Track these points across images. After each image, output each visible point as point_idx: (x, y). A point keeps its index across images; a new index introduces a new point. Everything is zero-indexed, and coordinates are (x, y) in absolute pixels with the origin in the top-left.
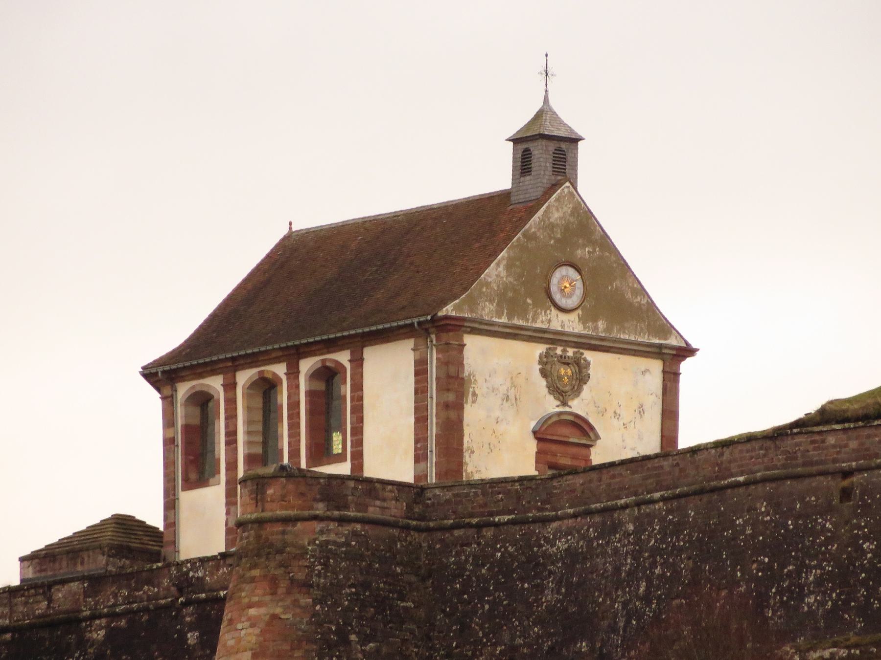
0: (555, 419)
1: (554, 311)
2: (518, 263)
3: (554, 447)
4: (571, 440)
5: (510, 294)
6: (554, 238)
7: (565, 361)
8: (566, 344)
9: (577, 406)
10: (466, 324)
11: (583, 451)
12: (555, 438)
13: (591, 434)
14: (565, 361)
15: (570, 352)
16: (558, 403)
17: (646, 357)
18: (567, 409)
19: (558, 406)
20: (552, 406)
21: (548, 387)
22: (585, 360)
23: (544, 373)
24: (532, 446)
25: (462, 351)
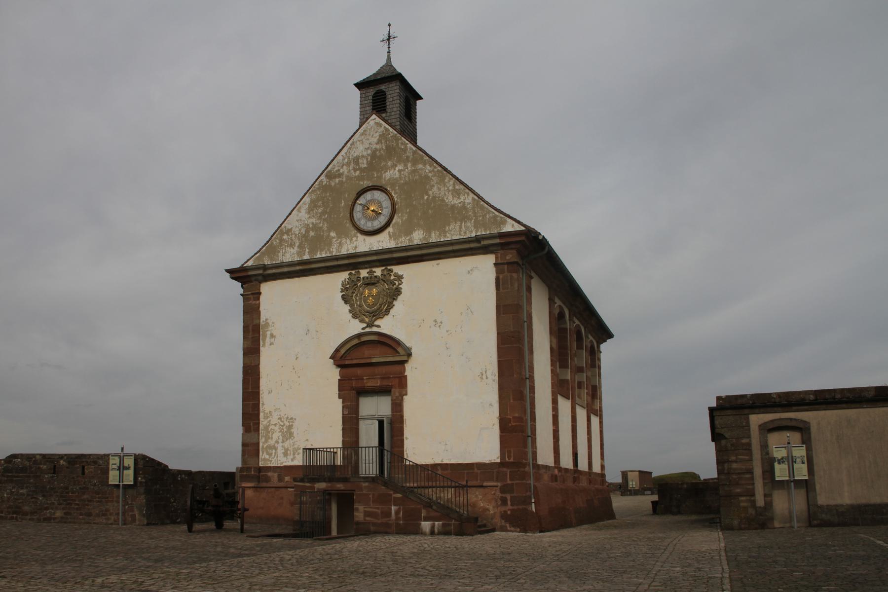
0: (356, 342)
1: (361, 237)
2: (320, 203)
3: (359, 371)
4: (374, 360)
5: (312, 234)
6: (360, 169)
7: (370, 283)
8: (370, 264)
9: (386, 326)
10: (250, 273)
11: (396, 368)
12: (355, 362)
13: (400, 350)
14: (370, 283)
15: (378, 272)
16: (365, 325)
17: (472, 255)
18: (375, 329)
19: (363, 329)
20: (356, 327)
21: (350, 311)
22: (396, 275)
23: (346, 299)
24: (334, 374)
25: (259, 299)
